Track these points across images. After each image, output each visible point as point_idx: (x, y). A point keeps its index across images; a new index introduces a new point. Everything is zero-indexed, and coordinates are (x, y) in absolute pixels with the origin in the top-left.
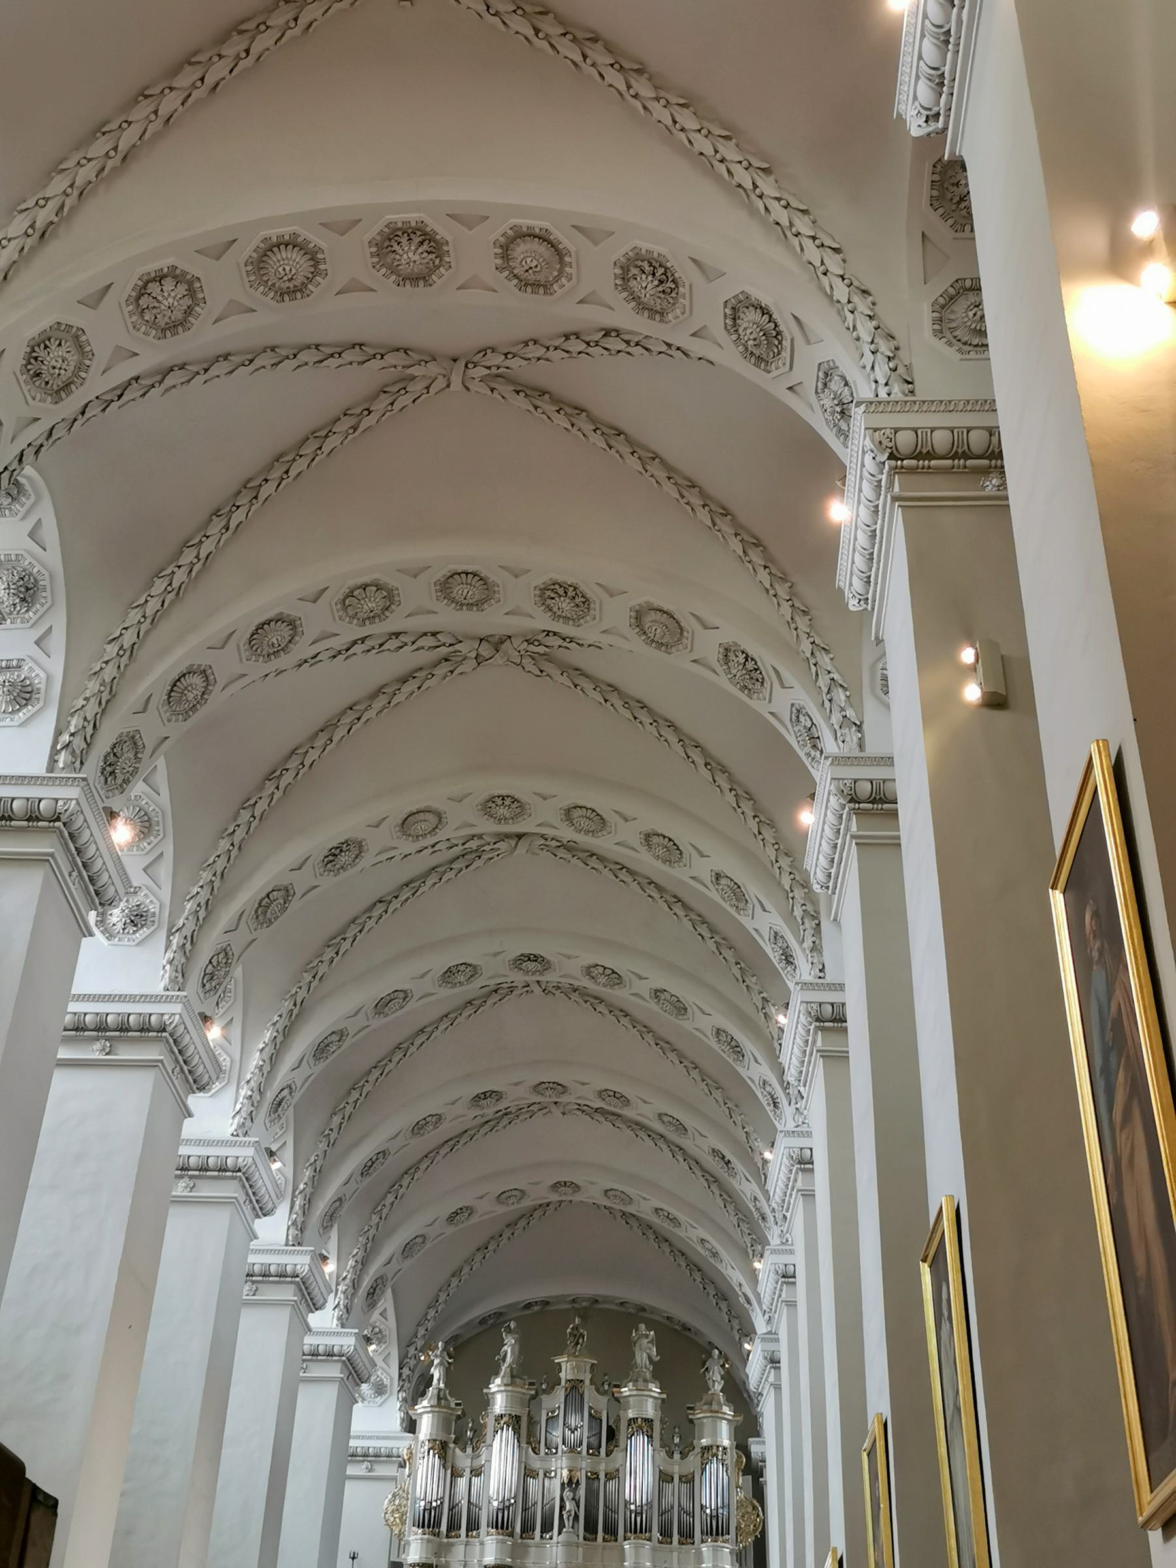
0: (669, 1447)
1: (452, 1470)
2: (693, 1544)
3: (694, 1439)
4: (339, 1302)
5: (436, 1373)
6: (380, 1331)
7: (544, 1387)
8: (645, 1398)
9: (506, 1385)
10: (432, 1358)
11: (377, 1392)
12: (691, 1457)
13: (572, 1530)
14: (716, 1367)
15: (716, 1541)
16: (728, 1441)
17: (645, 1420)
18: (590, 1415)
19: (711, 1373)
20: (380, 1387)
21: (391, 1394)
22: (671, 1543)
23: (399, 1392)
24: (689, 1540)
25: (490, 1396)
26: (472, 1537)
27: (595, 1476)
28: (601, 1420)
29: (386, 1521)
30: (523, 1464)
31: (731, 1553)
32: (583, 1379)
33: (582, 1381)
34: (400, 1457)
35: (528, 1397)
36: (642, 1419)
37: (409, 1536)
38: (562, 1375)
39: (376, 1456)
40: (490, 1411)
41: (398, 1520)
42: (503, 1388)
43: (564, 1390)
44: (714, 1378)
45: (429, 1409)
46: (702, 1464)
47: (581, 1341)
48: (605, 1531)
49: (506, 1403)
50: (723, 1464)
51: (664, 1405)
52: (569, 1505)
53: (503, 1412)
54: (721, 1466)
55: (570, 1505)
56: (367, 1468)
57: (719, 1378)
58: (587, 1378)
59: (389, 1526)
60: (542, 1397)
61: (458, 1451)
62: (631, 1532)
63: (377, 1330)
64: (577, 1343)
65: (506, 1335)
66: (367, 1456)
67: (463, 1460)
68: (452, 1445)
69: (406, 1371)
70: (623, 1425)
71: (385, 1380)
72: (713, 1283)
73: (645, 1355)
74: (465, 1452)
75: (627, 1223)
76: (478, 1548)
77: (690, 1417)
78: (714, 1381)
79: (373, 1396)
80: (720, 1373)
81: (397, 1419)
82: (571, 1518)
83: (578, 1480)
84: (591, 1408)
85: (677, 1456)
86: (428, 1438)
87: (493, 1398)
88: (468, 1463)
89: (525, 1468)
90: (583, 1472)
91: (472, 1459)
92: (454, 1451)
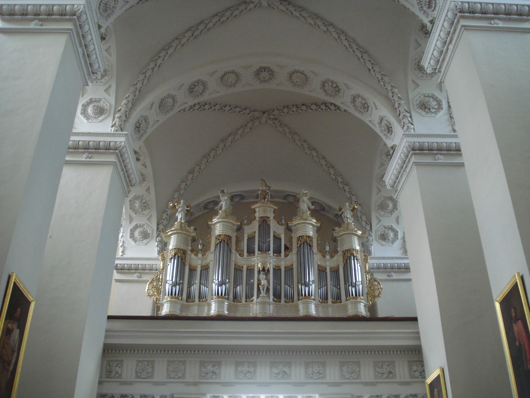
1: (189, 267)
2: (341, 302)
3: (338, 247)
4: (115, 123)
5: (179, 216)
6: (146, 201)
7: (245, 222)
8: (307, 225)
10: (177, 208)
11: (144, 237)
12: (335, 258)
13: (266, 296)
14: (348, 211)
15: (356, 299)
17: (309, 237)
18: (274, 236)
19: (346, 214)
20: (146, 234)
21: (152, 238)
22: (327, 303)
23: (157, 237)
24: (338, 301)
25: (212, 227)
26: (202, 301)
27: (278, 268)
28: (280, 239)
29: (148, 294)
31: (365, 306)
32: (269, 216)
33: (268, 217)
34: (157, 270)
35: (235, 227)
37: (163, 300)
38: (257, 215)
39: (143, 270)
40: (212, 234)
41: (156, 293)
42: (220, 220)
46: (344, 259)
47: (267, 196)
48: (286, 296)
50: (357, 259)
51: (318, 230)
52: (264, 282)
54: (356, 261)
55: (263, 281)
56: (137, 276)
57: (350, 217)
58: (271, 215)
59: (150, 296)
60: (244, 227)
61: (193, 256)
62: (302, 295)
63: (144, 201)
64: (265, 198)
65: (222, 196)
66: (138, 270)
67: (197, 261)
68: (189, 252)
69: (161, 227)
70: (295, 241)
71: (149, 231)
72: (341, 176)
73: (306, 204)
74: (198, 256)
75: (293, 138)
76: (206, 307)
77: (335, 235)
78: (347, 217)
79: (141, 239)
80: (350, 214)
81: (155, 251)
82: (265, 289)
83: (268, 269)
84: (274, 232)
85: (328, 257)
86: (175, 247)
87: (215, 228)
89: (235, 265)
90: (271, 265)
91: (202, 260)
92: (190, 256)
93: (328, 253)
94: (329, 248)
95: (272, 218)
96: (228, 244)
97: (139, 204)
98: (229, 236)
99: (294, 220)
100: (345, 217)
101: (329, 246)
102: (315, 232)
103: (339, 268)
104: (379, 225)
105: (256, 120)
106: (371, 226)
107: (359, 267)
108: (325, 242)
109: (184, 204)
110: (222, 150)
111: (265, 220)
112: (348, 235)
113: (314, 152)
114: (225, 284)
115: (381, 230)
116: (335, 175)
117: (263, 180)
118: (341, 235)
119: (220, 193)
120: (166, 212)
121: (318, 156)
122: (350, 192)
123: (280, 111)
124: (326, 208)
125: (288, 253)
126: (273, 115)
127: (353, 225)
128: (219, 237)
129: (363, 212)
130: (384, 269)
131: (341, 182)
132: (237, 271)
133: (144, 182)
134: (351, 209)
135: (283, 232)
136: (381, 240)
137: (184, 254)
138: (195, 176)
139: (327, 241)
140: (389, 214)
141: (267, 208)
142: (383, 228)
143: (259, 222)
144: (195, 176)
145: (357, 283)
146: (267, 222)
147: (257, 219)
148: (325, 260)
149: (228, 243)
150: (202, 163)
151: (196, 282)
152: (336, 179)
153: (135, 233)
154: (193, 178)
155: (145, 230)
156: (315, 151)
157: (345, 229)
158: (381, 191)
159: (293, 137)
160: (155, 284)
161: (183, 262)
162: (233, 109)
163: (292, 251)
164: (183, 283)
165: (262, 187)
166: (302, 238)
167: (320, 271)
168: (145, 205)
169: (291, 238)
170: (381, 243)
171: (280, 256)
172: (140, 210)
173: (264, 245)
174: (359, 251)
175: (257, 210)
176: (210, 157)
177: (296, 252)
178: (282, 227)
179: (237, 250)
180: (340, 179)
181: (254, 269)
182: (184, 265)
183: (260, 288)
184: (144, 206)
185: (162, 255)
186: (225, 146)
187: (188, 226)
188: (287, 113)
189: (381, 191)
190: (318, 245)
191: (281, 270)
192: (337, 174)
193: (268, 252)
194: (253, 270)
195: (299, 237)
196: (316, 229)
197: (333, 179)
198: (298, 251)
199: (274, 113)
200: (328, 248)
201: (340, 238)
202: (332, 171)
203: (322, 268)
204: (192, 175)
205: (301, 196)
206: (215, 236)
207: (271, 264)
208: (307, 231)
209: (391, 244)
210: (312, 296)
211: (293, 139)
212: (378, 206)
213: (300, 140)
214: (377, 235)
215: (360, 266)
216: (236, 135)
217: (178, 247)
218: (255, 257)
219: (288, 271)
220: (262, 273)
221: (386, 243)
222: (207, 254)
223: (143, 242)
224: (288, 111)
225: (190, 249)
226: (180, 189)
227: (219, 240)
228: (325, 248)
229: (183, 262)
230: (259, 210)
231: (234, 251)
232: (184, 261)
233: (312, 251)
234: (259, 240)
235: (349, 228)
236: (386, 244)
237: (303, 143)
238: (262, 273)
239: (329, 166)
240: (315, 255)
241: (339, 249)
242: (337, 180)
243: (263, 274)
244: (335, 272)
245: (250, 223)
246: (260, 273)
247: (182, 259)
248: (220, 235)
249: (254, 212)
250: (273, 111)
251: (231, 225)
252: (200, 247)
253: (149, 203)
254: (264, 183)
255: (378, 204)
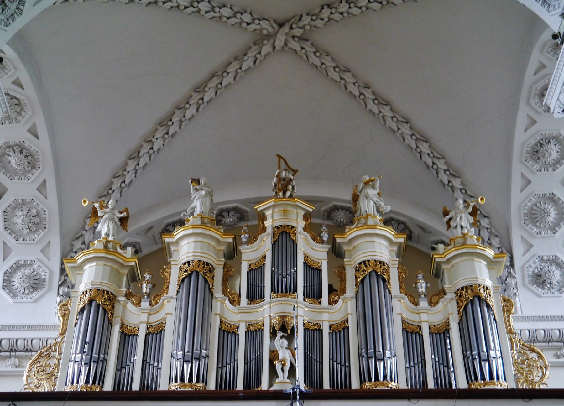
0: (412, 296)
6: (37, 213)
7: (244, 238)
8: (376, 239)
9: (194, 227)
12: (440, 306)
13: (288, 381)
16: (491, 282)
19: (458, 219)
25: (172, 248)
28: (320, 271)
30: (218, 317)
32: (295, 225)
33: (293, 227)
35: (223, 248)
36: (375, 260)
38: (268, 223)
40: (172, 263)
43: (270, 237)
44: (462, 224)
45: (93, 251)
47: (290, 187)
49: (195, 247)
52: (284, 354)
53: (190, 259)
55: (283, 353)
57: (468, 226)
58: (301, 224)
60: (240, 247)
61: (130, 305)
62: (370, 380)
63: (34, 211)
68: (122, 299)
70: (350, 274)
71: (43, 274)
73: (372, 203)
74: (140, 306)
77: (437, 260)
78: (462, 227)
79: (27, 292)
80: (468, 221)
82: (287, 368)
84: (306, 257)
85: (424, 304)
86: (90, 287)
88: (144, 318)
91: (149, 314)
92: (125, 306)
93: (423, 296)
94: (427, 288)
95: (300, 229)
96: (206, 281)
97: (22, 217)
98: (208, 264)
99: (346, 230)
100: (457, 226)
101: (427, 284)
102: (394, 254)
103: (449, 326)
104: (528, 255)
105: (265, 42)
106: (512, 258)
107: (493, 323)
108: (417, 276)
109: (113, 209)
110: (197, 110)
111: (286, 232)
112: (465, 258)
113: (387, 108)
114: (199, 359)
115: (533, 265)
116: (431, 155)
117: (279, 156)
118: (449, 260)
119: (191, 182)
120: (81, 239)
121: (394, 117)
122: (463, 191)
123: (314, 18)
124: (416, 231)
125: (337, 297)
126: (300, 28)
127: (476, 241)
128: (187, 265)
129: (493, 231)
130: (545, 342)
131: (445, 171)
132: (226, 334)
133: (34, 171)
134: (470, 210)
135: (326, 257)
136: (535, 286)
137: (110, 300)
138: (141, 164)
139: (419, 273)
140: (549, 232)
141: (290, 209)
142: (537, 261)
143: (274, 237)
144: (141, 164)
145: (492, 353)
146: (290, 236)
147: (269, 230)
148: (419, 310)
149: (206, 277)
150: (156, 137)
151: (136, 358)
152: (434, 164)
153: (14, 279)
154: (137, 167)
155: (35, 273)
156: (389, 107)
157: (458, 245)
158: (530, 182)
159: (343, 76)
160: (44, 365)
161: (108, 318)
162: (217, 10)
163: (344, 291)
164: (105, 360)
165: (279, 169)
166: (366, 266)
167: (407, 332)
168: (37, 220)
169: (344, 268)
170: (535, 290)
171: (320, 303)
172: (26, 231)
173: (284, 280)
174: (492, 290)
175: (268, 213)
176: (173, 123)
177: (353, 295)
178: (323, 246)
179: (224, 292)
180: (441, 165)
181: (263, 330)
182: (111, 324)
183: (275, 366)
184: (35, 224)
185: (64, 305)
186: (202, 99)
187: (121, 248)
188: (330, 19)
189: (530, 182)
190: (401, 281)
191: (322, 330)
192: (436, 154)
193: (294, 293)
194: (261, 331)
195: (360, 263)
196: (396, 248)
197: (428, 167)
198: (357, 292)
199: (301, 24)
200: (424, 285)
201: (449, 266)
202: (425, 148)
203: (412, 327)
204: (135, 163)
205: (362, 189)
206: (179, 266)
207: (299, 317)
208: (377, 250)
209: (556, 293)
210: (391, 380)
211: (343, 82)
212: (525, 215)
213: (357, 84)
214: (526, 276)
215: (495, 319)
216: (225, 74)
217: (98, 287)
218: (265, 304)
219: (338, 334)
220: (279, 334)
221: (546, 291)
222: (160, 302)
223: (31, 296)
224: (331, 13)
225: (125, 292)
226: (110, 191)
227: (186, 271)
228: (416, 288)
229: (108, 318)
230: (273, 213)
231: (218, 294)
232: (110, 314)
233: (390, 292)
234: (272, 272)
235: (469, 242)
236: (547, 293)
237: (363, 91)
238: (279, 334)
239: (418, 136)
240: (395, 301)
241: (447, 287)
242: (435, 167)
243: (282, 337)
244: (440, 334)
245: (252, 240)
246: (276, 336)
247: (105, 311)
248: (189, 262)
249: (262, 217)
250: (300, 19)
251: (213, 243)
252: (145, 288)
253: (43, 216)
254: (282, 162)
255: (526, 211)
